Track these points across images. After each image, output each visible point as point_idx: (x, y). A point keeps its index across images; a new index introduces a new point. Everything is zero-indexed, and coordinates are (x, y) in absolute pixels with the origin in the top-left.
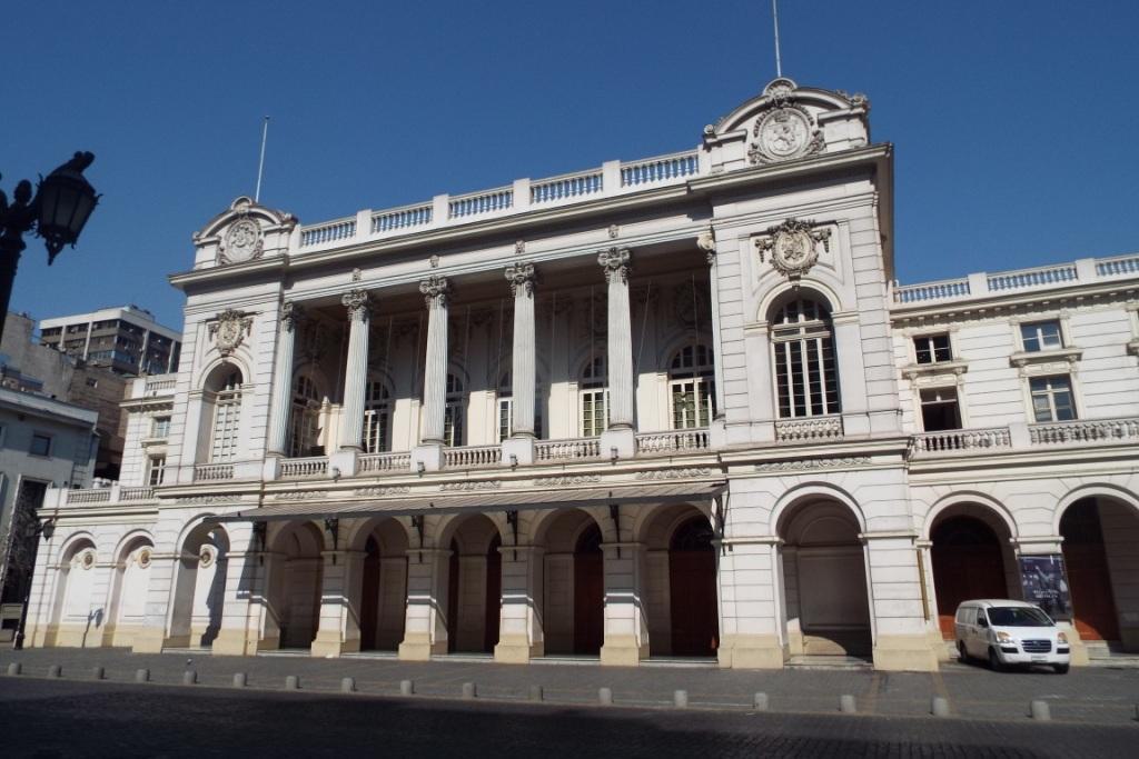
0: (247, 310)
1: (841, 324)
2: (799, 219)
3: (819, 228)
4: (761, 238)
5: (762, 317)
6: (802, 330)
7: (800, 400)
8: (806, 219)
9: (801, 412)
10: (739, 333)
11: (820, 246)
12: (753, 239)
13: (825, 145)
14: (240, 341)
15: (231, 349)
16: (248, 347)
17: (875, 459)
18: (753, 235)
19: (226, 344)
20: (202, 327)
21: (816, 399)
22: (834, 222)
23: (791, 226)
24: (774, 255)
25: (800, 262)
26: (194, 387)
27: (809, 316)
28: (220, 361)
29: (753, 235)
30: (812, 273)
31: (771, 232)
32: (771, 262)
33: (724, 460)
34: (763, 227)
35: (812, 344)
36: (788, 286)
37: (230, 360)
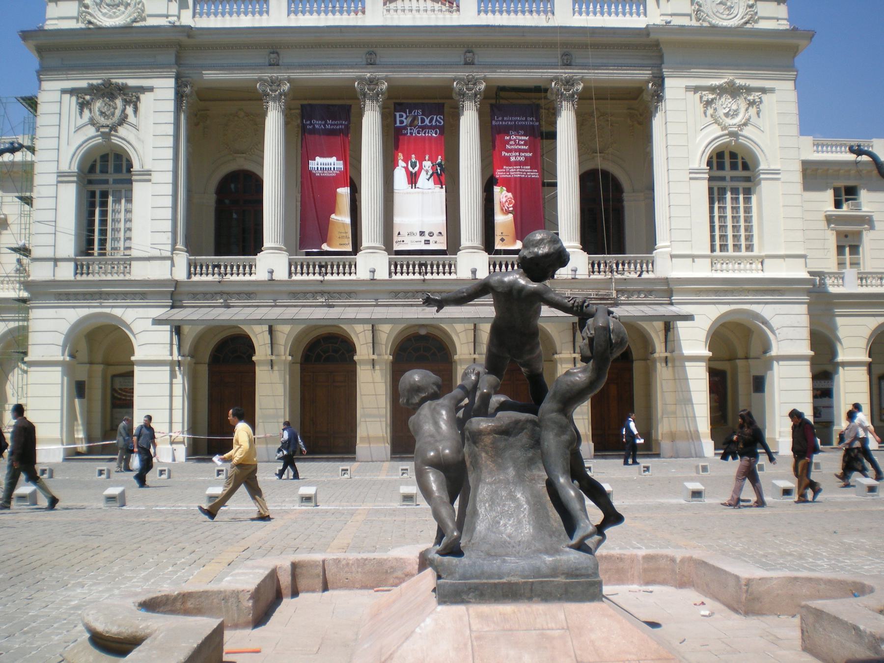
0: (131, 83)
5: (704, 166)
6: (728, 178)
7: (723, 237)
9: (724, 247)
11: (753, 111)
14: (123, 120)
15: (114, 128)
16: (135, 127)
19: (109, 122)
20: (67, 97)
24: (715, 109)
25: (737, 120)
26: (64, 167)
28: (99, 140)
29: (696, 89)
32: (712, 116)
37: (115, 140)
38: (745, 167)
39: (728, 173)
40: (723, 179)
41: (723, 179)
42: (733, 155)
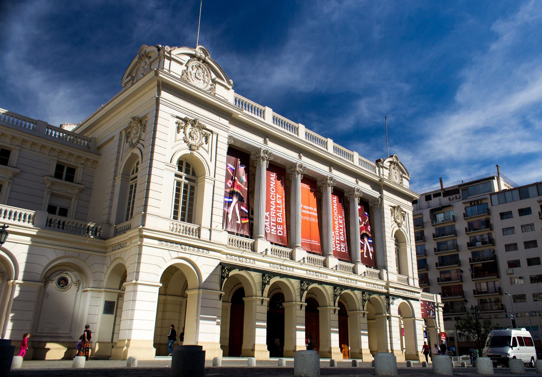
1: (208, 182)
2: (200, 122)
3: (206, 131)
4: (181, 121)
6: (184, 177)
8: (203, 123)
10: (163, 166)
12: (176, 120)
13: (215, 94)
17: (211, 253)
18: (177, 117)
21: (183, 215)
22: (212, 132)
23: (194, 123)
27: (187, 172)
29: (177, 117)
30: (201, 150)
31: (186, 120)
33: (144, 233)
34: (183, 116)
35: (186, 186)
36: (189, 152)
38: (194, 174)
39: (184, 174)
40: (181, 177)
41: (181, 177)
42: (188, 165)
